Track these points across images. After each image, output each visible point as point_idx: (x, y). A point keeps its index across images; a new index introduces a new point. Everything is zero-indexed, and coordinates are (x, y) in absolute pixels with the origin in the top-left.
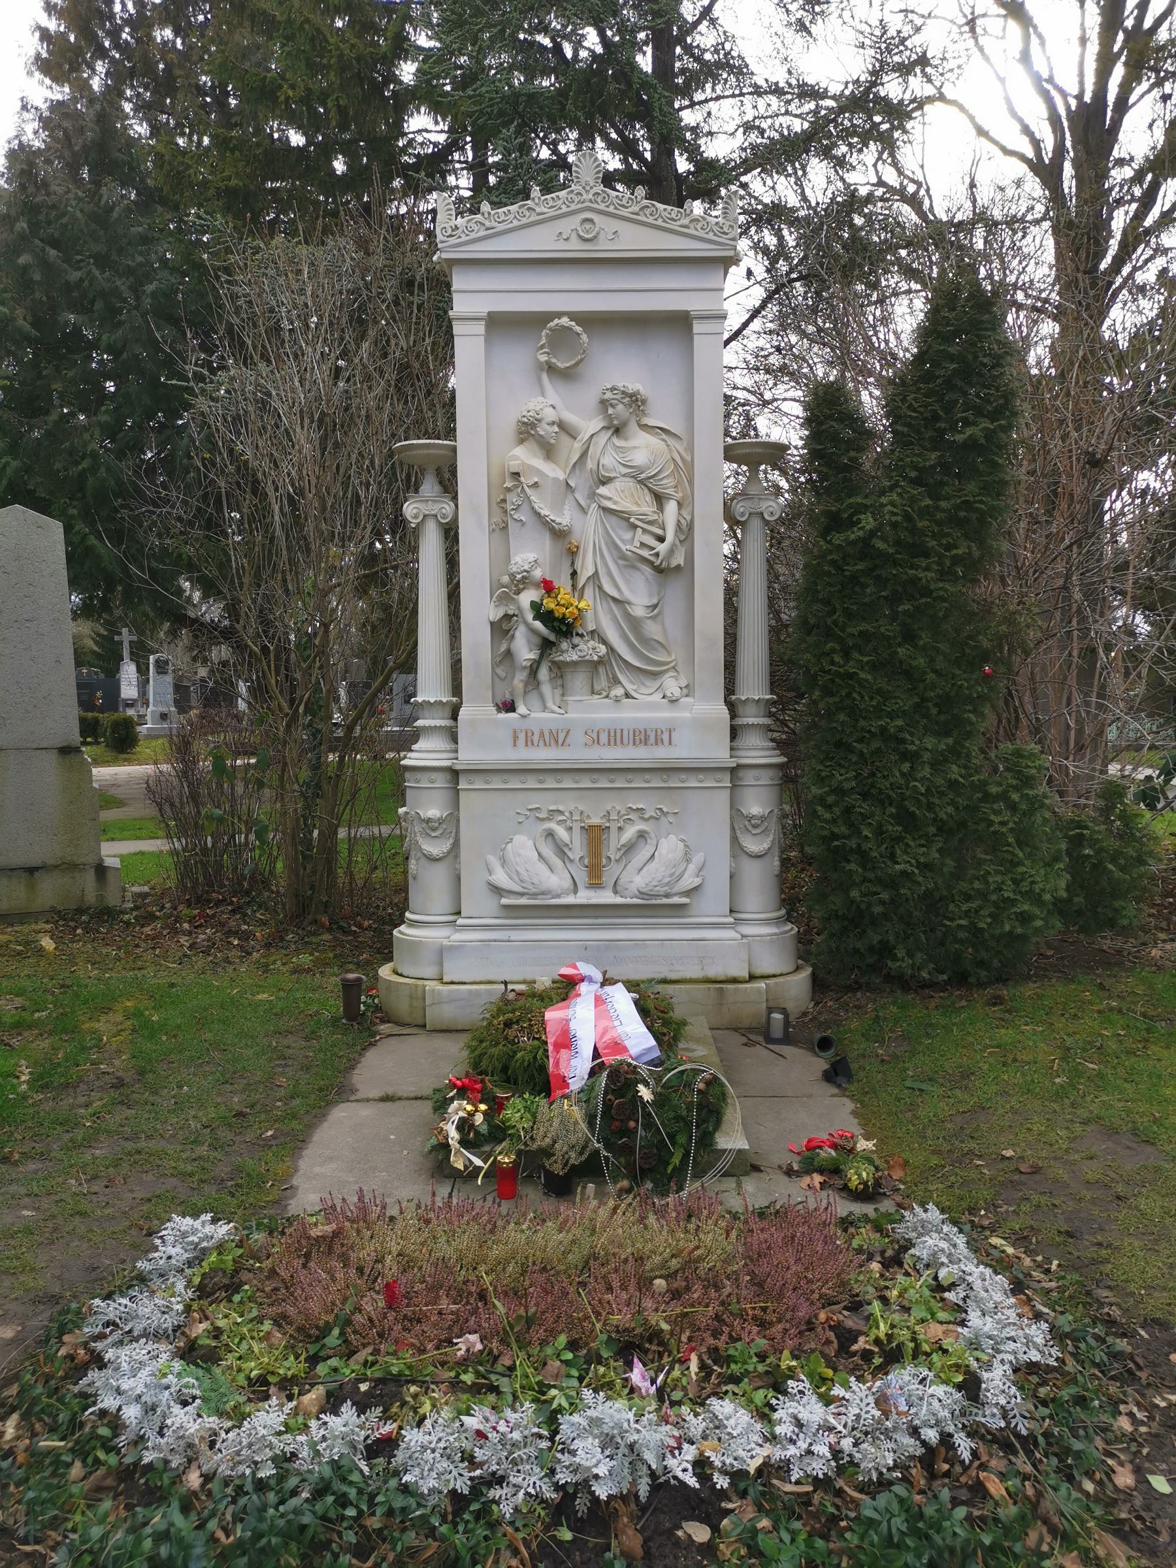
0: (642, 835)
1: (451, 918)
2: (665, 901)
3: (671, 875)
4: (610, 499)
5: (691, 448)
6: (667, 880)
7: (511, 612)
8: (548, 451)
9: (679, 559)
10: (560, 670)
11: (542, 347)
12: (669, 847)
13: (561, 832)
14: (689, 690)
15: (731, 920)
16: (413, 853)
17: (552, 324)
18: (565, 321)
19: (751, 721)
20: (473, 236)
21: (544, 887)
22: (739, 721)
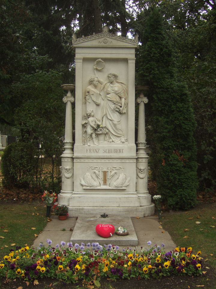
0: (116, 173)
1: (71, 192)
2: (121, 188)
3: (122, 183)
4: (109, 98)
5: (128, 87)
6: (121, 183)
7: (86, 122)
8: (95, 87)
9: (125, 111)
10: (97, 135)
11: (95, 65)
12: (122, 176)
13: (97, 172)
14: (127, 140)
15: (136, 193)
16: (63, 177)
17: (97, 60)
18: (100, 60)
19: (141, 147)
20: (80, 42)
21: (93, 185)
22: (138, 147)
